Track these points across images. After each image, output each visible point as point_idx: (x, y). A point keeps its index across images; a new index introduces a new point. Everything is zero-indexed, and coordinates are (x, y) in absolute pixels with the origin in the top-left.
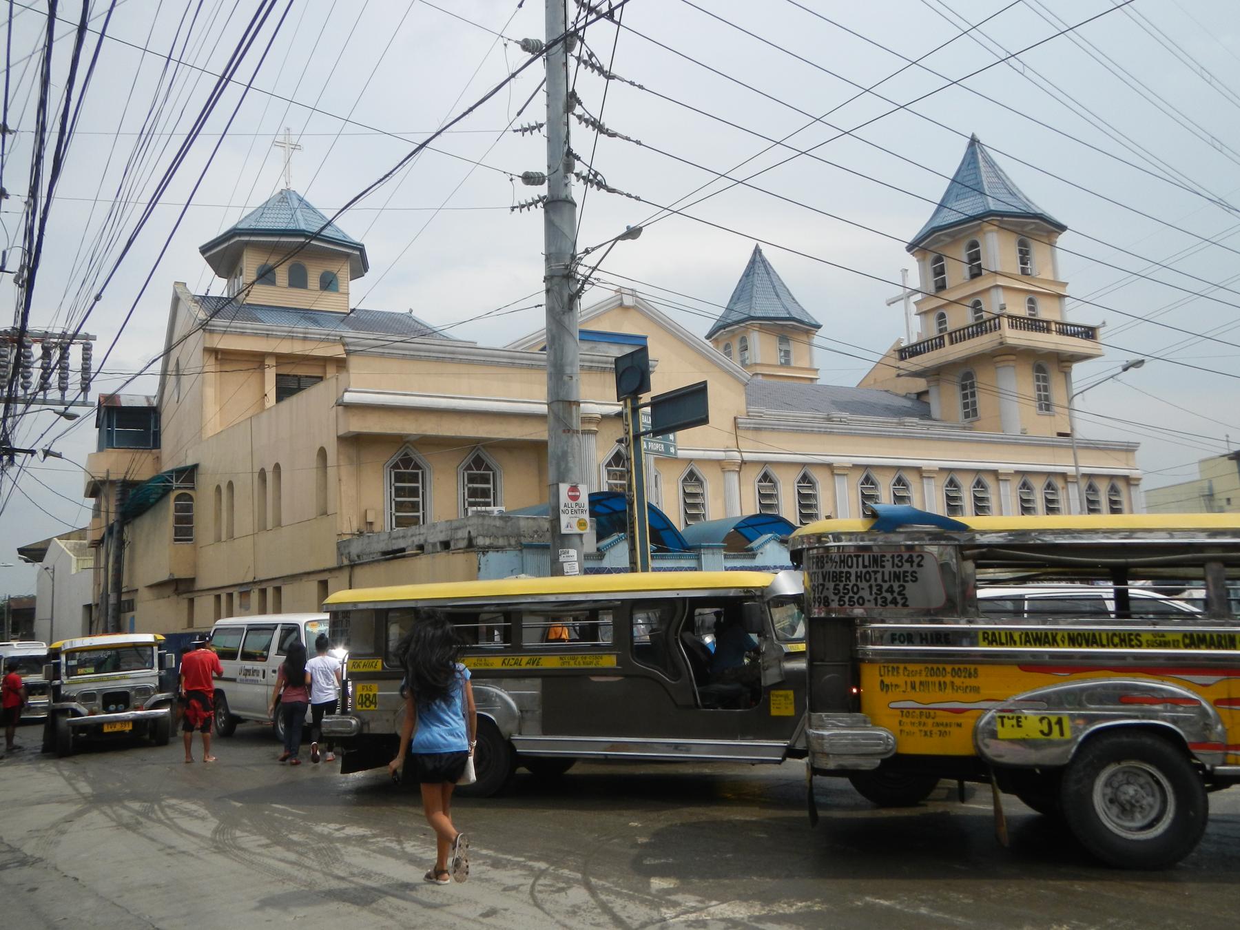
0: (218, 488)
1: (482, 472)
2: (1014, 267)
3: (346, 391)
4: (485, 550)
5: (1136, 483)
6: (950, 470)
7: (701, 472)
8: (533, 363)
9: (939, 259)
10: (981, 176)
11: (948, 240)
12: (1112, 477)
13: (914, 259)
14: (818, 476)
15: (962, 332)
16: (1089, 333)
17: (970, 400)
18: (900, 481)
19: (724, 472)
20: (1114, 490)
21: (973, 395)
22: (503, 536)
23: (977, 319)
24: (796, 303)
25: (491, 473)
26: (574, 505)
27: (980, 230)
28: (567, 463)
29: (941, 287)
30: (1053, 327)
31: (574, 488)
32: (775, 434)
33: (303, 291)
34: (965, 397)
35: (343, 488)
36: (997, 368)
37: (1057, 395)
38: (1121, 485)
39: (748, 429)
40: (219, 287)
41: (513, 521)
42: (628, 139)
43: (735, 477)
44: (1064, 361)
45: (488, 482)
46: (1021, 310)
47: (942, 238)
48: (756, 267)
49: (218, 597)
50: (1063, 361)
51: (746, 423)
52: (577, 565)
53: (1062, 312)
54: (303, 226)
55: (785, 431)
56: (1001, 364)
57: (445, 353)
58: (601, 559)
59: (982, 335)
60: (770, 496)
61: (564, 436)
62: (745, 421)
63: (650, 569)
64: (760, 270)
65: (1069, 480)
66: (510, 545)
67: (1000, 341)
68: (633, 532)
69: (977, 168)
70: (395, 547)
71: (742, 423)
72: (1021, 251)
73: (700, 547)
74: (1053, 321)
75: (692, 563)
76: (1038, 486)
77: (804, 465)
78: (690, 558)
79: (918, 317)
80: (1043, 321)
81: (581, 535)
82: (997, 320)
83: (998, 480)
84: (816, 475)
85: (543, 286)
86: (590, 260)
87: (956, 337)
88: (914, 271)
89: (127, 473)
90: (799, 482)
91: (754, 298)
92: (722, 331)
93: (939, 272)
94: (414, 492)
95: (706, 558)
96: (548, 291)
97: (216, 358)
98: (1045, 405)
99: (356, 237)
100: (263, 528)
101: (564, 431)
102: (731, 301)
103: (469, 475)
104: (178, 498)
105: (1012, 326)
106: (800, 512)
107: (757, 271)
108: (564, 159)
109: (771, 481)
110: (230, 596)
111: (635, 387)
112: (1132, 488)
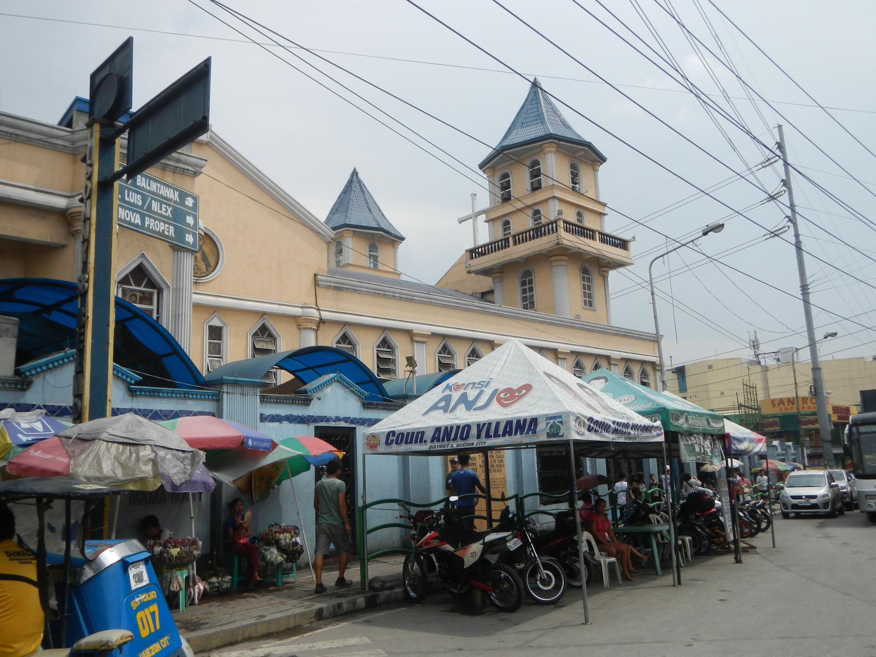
7: (275, 327)
9: (506, 176)
10: (542, 110)
12: (643, 362)
15: (524, 235)
16: (623, 244)
17: (528, 294)
19: (300, 329)
21: (531, 289)
24: (385, 218)
27: (541, 150)
32: (356, 297)
34: (524, 291)
38: (649, 370)
39: (329, 287)
44: (604, 265)
46: (573, 219)
48: (353, 185)
50: (602, 267)
51: (326, 281)
53: (602, 225)
55: (366, 293)
56: (553, 264)
58: (23, 390)
63: (109, 412)
64: (355, 187)
65: (612, 362)
67: (556, 241)
68: (83, 342)
69: (539, 103)
71: (323, 281)
72: (572, 173)
74: (598, 231)
75: (209, 406)
77: (384, 329)
78: (203, 398)
79: (487, 224)
80: (590, 230)
82: (554, 225)
84: (396, 340)
90: (379, 346)
91: (350, 210)
93: (506, 186)
95: (231, 400)
98: (589, 302)
102: (330, 213)
105: (567, 230)
107: (353, 189)
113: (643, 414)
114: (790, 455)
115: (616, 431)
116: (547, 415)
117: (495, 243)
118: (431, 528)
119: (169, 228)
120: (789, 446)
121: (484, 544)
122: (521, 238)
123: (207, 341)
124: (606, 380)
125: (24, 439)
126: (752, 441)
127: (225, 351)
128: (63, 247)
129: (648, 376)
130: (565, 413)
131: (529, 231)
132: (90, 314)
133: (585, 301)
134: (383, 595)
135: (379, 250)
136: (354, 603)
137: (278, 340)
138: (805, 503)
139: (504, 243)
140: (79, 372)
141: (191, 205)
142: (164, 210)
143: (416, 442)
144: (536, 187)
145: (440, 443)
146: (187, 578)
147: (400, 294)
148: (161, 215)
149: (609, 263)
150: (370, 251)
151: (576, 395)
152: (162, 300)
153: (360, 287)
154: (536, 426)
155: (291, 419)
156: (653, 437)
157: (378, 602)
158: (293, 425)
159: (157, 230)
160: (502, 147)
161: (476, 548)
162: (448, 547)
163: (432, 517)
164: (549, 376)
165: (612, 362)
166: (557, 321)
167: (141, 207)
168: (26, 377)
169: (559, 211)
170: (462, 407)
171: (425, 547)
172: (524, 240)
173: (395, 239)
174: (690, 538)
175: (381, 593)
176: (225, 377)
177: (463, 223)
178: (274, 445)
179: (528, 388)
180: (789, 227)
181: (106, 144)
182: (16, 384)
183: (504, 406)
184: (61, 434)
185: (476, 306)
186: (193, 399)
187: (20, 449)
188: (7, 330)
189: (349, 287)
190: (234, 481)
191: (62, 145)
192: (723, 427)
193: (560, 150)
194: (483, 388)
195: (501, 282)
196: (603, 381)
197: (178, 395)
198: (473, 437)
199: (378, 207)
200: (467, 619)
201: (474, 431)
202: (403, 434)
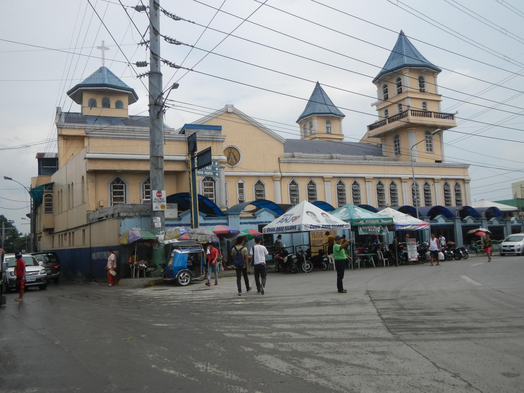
0: (59, 192)
3: (88, 153)
4: (124, 218)
5: (467, 182)
7: (264, 181)
8: (170, 139)
9: (386, 86)
11: (389, 77)
12: (456, 179)
16: (451, 116)
18: (355, 183)
19: (273, 181)
20: (457, 185)
21: (399, 145)
22: (132, 212)
23: (400, 111)
26: (159, 199)
27: (401, 73)
28: (156, 181)
29: (386, 98)
30: (433, 114)
31: (159, 192)
32: (298, 164)
33: (108, 109)
34: (396, 146)
35: (89, 192)
37: (435, 144)
38: (461, 183)
39: (285, 162)
40: (76, 108)
42: (187, 45)
43: (278, 183)
47: (386, 77)
49: (59, 235)
51: (284, 160)
52: (160, 224)
54: (106, 82)
57: (131, 136)
58: (180, 220)
60: (295, 191)
61: (155, 171)
62: (283, 159)
65: (435, 181)
66: (136, 216)
68: (191, 209)
69: (402, 45)
70: (101, 216)
75: (225, 221)
77: (310, 177)
78: (223, 219)
81: (163, 212)
82: (407, 112)
84: (315, 181)
85: (148, 108)
86: (164, 96)
88: (373, 90)
89: (36, 186)
92: (302, 119)
93: (386, 92)
94: (121, 193)
96: (149, 111)
97: (64, 139)
98: (430, 148)
99: (131, 86)
100: (69, 208)
101: (155, 169)
103: (145, 185)
104: (46, 196)
105: (413, 115)
106: (309, 197)
108: (155, 56)
109: (296, 184)
110: (62, 235)
111: (193, 147)
112: (466, 184)
113: (344, 221)
123: (238, 189)
124: (347, 207)
125: (181, 233)
128: (186, 171)
129: (460, 186)
131: (397, 115)
135: (332, 124)
140: (192, 216)
141: (217, 164)
144: (400, 92)
146: (219, 264)
147: (317, 161)
155: (250, 223)
161: (286, 258)
162: (282, 258)
172: (394, 120)
173: (340, 117)
178: (239, 232)
179: (299, 216)
188: (175, 207)
190: (232, 241)
193: (411, 71)
195: (385, 141)
199: (331, 101)
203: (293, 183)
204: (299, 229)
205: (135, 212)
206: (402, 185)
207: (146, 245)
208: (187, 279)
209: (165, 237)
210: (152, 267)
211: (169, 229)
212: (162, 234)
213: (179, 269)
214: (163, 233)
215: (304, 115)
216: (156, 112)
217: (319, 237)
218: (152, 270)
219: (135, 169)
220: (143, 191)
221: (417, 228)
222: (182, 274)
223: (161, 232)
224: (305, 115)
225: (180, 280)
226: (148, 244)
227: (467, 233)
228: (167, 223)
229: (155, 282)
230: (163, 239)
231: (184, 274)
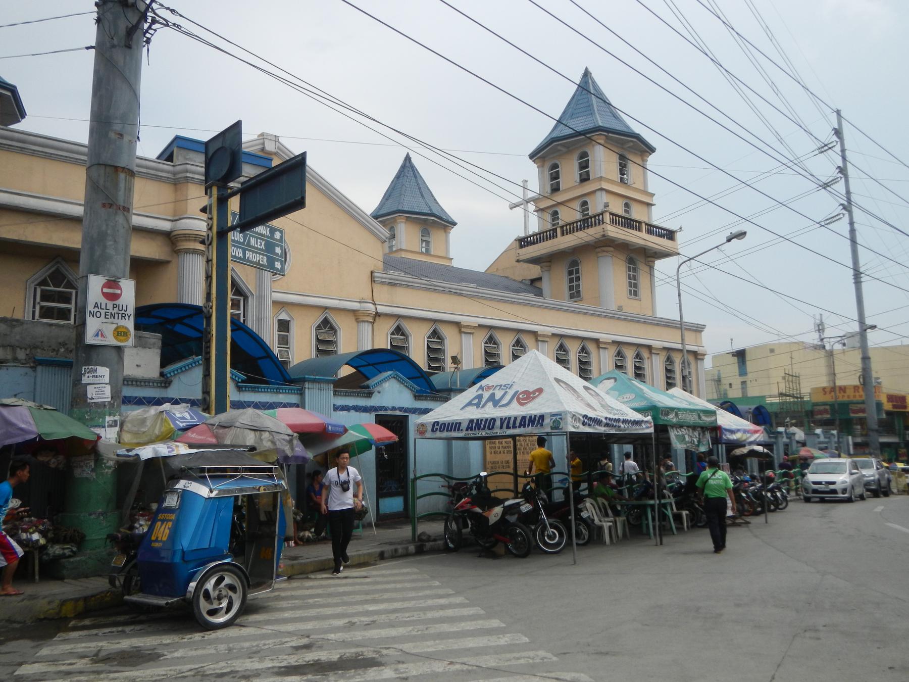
1: (61, 289)
2: (616, 176)
6: (562, 336)
7: (336, 320)
9: (555, 166)
11: (564, 149)
13: (535, 166)
14: (448, 333)
16: (670, 235)
17: (575, 284)
19: (358, 322)
21: (578, 279)
24: (437, 203)
25: (74, 292)
26: (110, 306)
28: (105, 247)
29: (556, 189)
30: (643, 225)
31: (113, 283)
32: (409, 291)
34: (571, 281)
36: (598, 257)
37: (643, 281)
39: (383, 283)
41: (25, 326)
43: (368, 328)
44: (650, 256)
45: (68, 301)
46: (620, 211)
47: (559, 148)
48: (406, 170)
51: (382, 278)
52: (108, 390)
53: (649, 215)
55: (418, 288)
56: (600, 255)
58: (166, 387)
59: (588, 228)
65: (653, 351)
66: (15, 359)
67: (602, 233)
68: (208, 353)
71: (379, 277)
72: (620, 164)
73: (302, 380)
74: (644, 222)
75: (294, 399)
76: (630, 354)
77: (435, 321)
78: (291, 392)
80: (636, 221)
81: (119, 350)
82: (601, 217)
83: (599, 347)
84: (446, 332)
87: (567, 229)
90: (429, 337)
93: (555, 177)
95: (312, 394)
96: (98, 21)
98: (634, 291)
101: (104, 205)
102: (384, 197)
103: (42, 291)
109: (403, 334)
111: (224, 172)
112: (699, 362)
113: (637, 410)
114: (833, 443)
115: (607, 425)
116: (551, 413)
117: (543, 233)
118: (465, 496)
119: (263, 258)
120: (833, 435)
121: (504, 507)
122: (569, 228)
124: (615, 379)
125: (182, 425)
126: (745, 431)
127: (292, 341)
128: (168, 262)
130: (564, 412)
131: (577, 222)
132: (214, 332)
133: (630, 291)
134: (429, 545)
135: (432, 236)
136: (407, 549)
137: (338, 331)
138: (824, 488)
139: (551, 234)
140: (207, 375)
142: (259, 244)
143: (455, 430)
144: (585, 179)
145: (473, 432)
148: (257, 248)
149: (655, 253)
150: (422, 236)
151: (579, 396)
152: (248, 306)
153: (412, 283)
154: (543, 420)
155: (357, 409)
156: (643, 429)
157: (425, 550)
158: (358, 413)
159: (255, 260)
160: (552, 139)
161: (498, 510)
162: (478, 510)
163: (467, 487)
164: (558, 381)
165: (653, 351)
166: (599, 312)
167: (243, 243)
168: (167, 377)
169: (605, 203)
170: (490, 404)
171: (461, 510)
172: (571, 232)
173: (446, 224)
174: (687, 512)
175: (427, 543)
176: (307, 376)
177: (514, 209)
178: (346, 430)
179: (540, 390)
180: (844, 214)
181: (222, 202)
182: (161, 383)
183: (522, 404)
184: (207, 422)
185: (521, 299)
186: (283, 393)
187: (180, 432)
188: (154, 344)
189: (403, 283)
191: (166, 177)
192: (716, 420)
194: (507, 390)
195: (549, 270)
196: (613, 380)
197: (272, 390)
198: (497, 428)
200: (490, 562)
201: (498, 423)
202: (445, 424)
203: (399, 330)
204: (556, 426)
205: (13, 348)
206: (599, 355)
207: (48, 462)
208: (231, 597)
209: (119, 434)
210: (67, 543)
211: (135, 413)
212: (110, 426)
213: (202, 557)
214: (115, 421)
215: (379, 214)
216: (123, 25)
217: (504, 452)
218: (66, 551)
219: (17, 238)
220: (34, 307)
221: (750, 437)
222: (213, 581)
223: (108, 418)
224: (381, 212)
225: (204, 606)
226: (53, 460)
227: (732, 454)
228: (128, 392)
229: (81, 604)
230: (113, 441)
231: (220, 580)
